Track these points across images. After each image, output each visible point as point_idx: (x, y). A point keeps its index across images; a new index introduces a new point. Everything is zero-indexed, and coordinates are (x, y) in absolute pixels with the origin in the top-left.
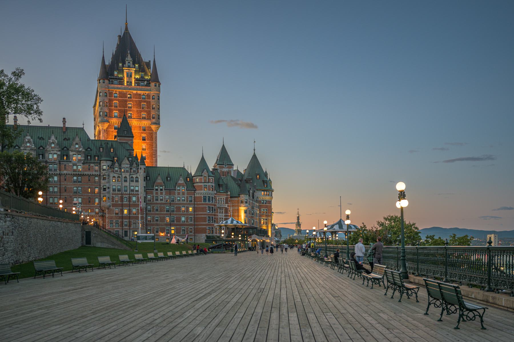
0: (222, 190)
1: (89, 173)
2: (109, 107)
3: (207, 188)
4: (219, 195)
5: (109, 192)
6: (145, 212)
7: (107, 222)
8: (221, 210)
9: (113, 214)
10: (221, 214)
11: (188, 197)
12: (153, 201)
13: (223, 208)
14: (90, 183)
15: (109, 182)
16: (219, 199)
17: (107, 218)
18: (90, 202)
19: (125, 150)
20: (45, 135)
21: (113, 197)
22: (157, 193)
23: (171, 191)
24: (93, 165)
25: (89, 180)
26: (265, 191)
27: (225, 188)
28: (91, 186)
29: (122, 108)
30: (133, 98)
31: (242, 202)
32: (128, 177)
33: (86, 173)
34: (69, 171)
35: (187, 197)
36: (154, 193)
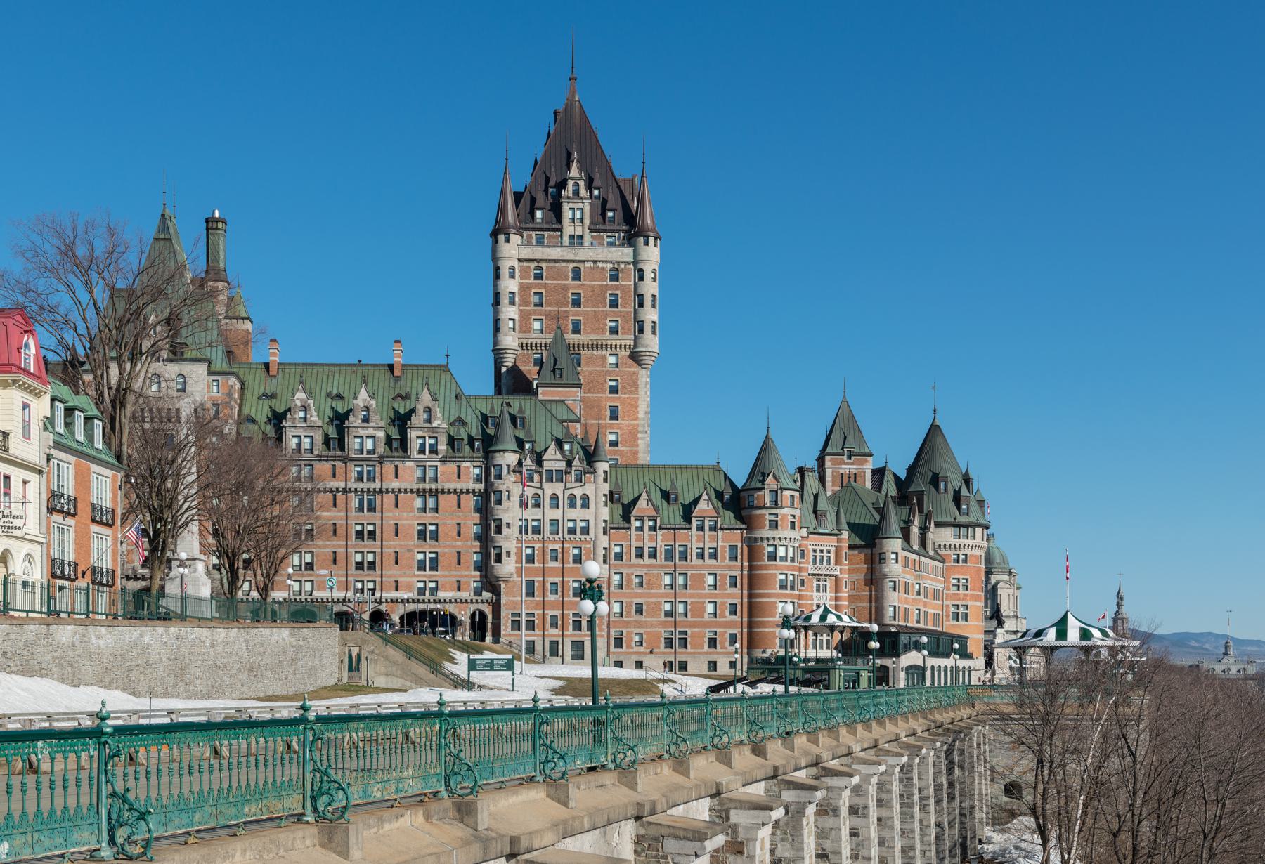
0: (826, 527)
2: (520, 305)
3: (779, 523)
8: (821, 583)
10: (821, 594)
11: (724, 547)
14: (459, 512)
16: (815, 551)
17: (504, 605)
19: (554, 421)
20: (347, 387)
24: (468, 464)
26: (963, 526)
27: (834, 519)
28: (462, 522)
30: (585, 280)
33: (452, 486)
34: (406, 481)
35: (723, 547)
36: (633, 537)
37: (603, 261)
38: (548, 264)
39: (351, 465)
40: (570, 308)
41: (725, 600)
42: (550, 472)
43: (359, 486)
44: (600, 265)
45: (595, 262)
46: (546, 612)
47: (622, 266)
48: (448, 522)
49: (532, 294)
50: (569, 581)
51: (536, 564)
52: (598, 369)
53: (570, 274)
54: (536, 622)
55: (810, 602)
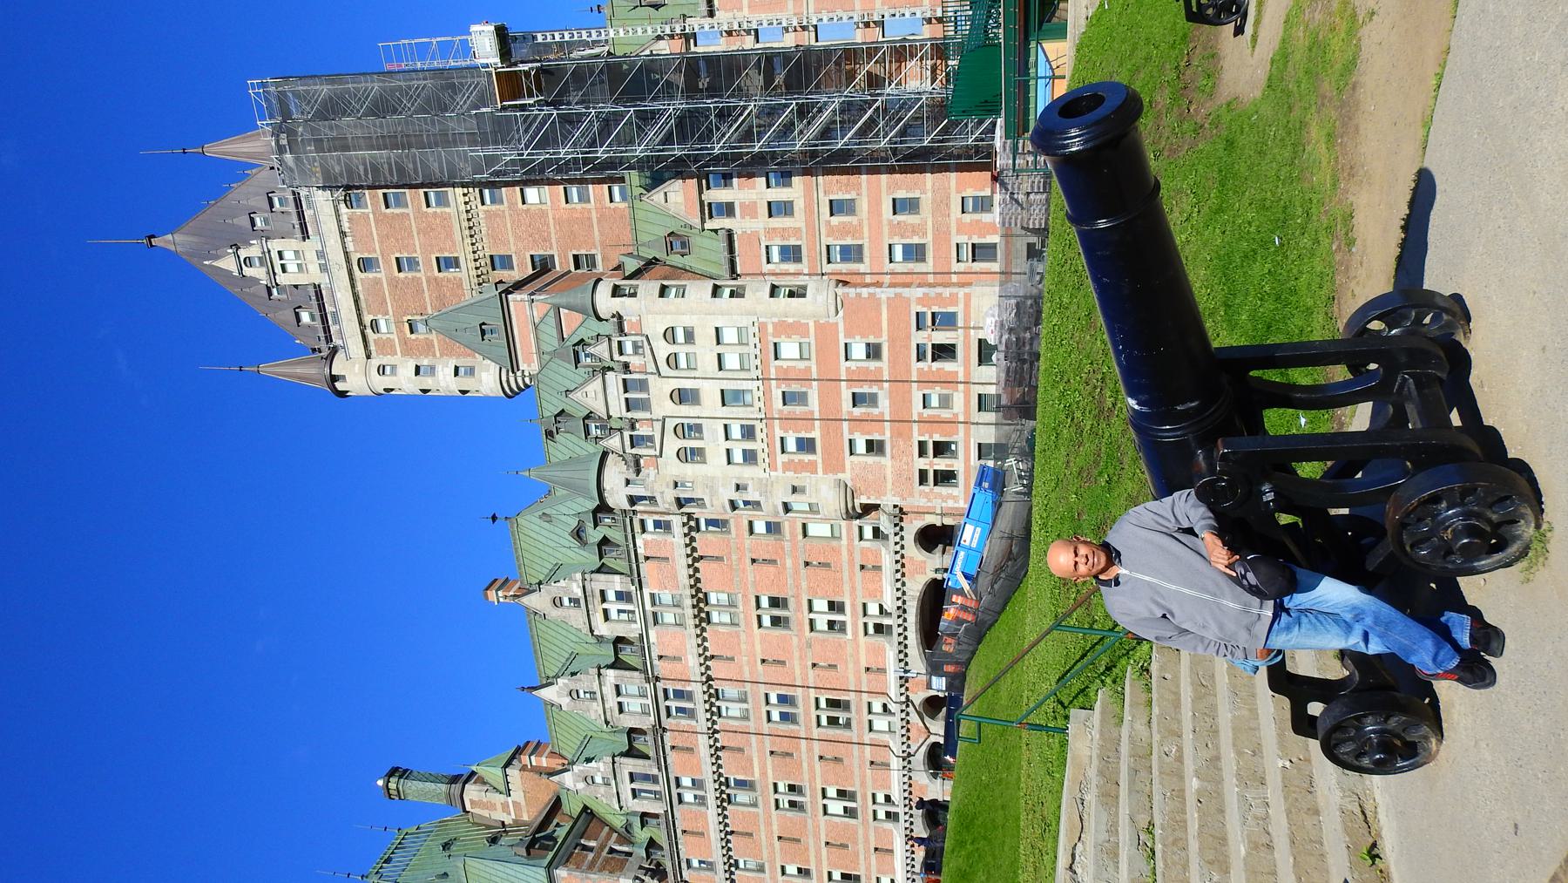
1: (681, 562)
2: (434, 355)
5: (765, 487)
6: (865, 292)
7: (929, 500)
9: (882, 467)
12: (798, 230)
14: (729, 559)
15: (711, 484)
18: (826, 565)
22: (751, 210)
24: (639, 542)
25: (719, 559)
28: (749, 556)
29: (427, 299)
33: (683, 573)
37: (339, 221)
38: (365, 313)
39: (666, 723)
42: (629, 405)
43: (702, 715)
44: (346, 226)
45: (343, 234)
46: (915, 418)
48: (751, 578)
49: (413, 336)
50: (848, 369)
51: (815, 434)
52: (509, 225)
53: (370, 275)
54: (937, 438)
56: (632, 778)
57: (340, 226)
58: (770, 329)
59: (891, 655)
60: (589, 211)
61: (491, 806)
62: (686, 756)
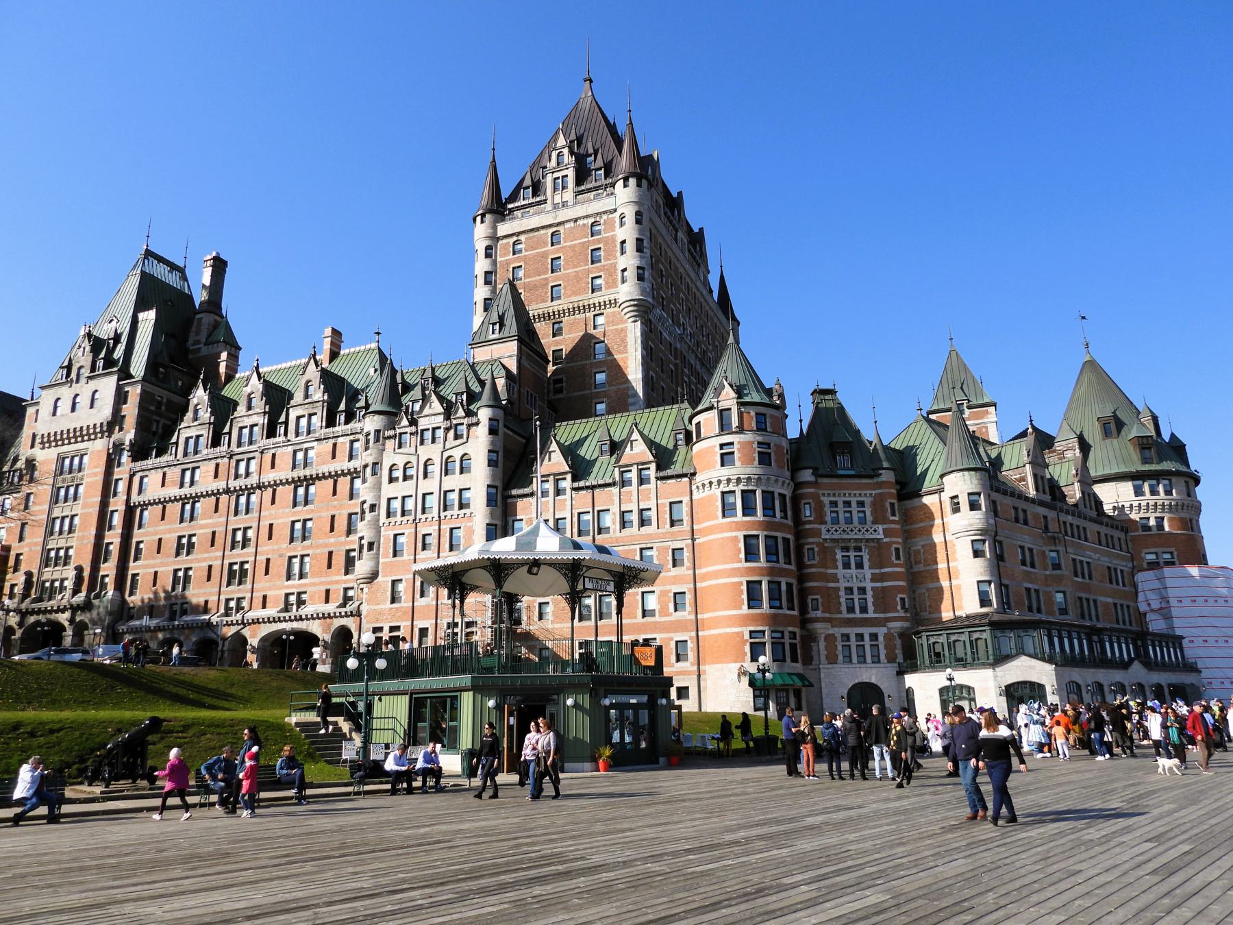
3: (737, 455)
4: (832, 487)
8: (852, 554)
9: (384, 602)
10: (853, 571)
11: (664, 505)
13: (863, 545)
14: (335, 500)
15: (378, 487)
18: (329, 566)
21: (387, 538)
23: (597, 491)
25: (335, 493)
31: (956, 509)
32: (437, 461)
33: (325, 469)
37: (583, 217)
38: (526, 236)
40: (549, 274)
41: (668, 588)
44: (581, 222)
45: (576, 220)
47: (605, 217)
55: (832, 585)
56: (198, 437)
57: (580, 218)
58: (469, 524)
59: (271, 612)
60: (590, 389)
61: (198, 333)
62: (213, 473)
